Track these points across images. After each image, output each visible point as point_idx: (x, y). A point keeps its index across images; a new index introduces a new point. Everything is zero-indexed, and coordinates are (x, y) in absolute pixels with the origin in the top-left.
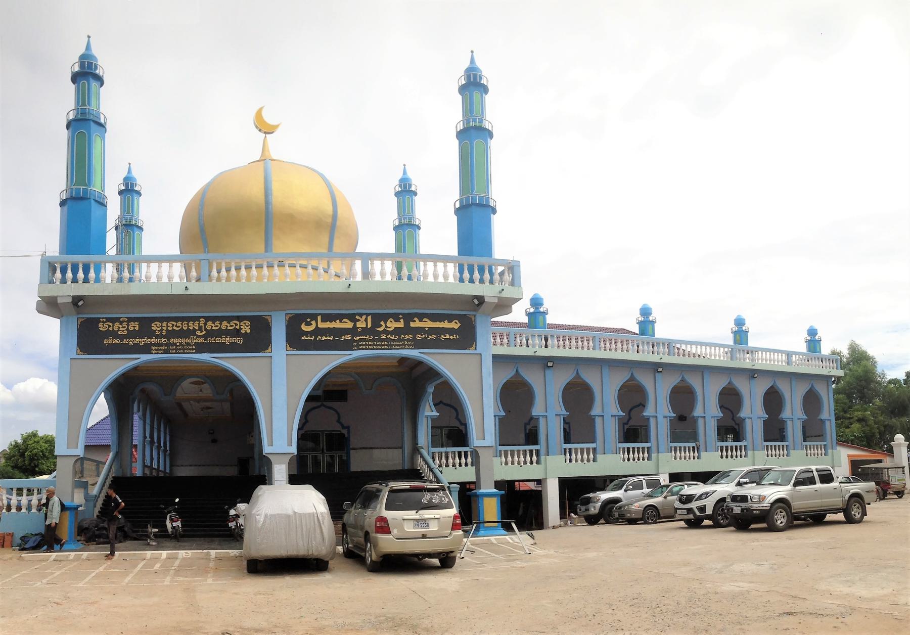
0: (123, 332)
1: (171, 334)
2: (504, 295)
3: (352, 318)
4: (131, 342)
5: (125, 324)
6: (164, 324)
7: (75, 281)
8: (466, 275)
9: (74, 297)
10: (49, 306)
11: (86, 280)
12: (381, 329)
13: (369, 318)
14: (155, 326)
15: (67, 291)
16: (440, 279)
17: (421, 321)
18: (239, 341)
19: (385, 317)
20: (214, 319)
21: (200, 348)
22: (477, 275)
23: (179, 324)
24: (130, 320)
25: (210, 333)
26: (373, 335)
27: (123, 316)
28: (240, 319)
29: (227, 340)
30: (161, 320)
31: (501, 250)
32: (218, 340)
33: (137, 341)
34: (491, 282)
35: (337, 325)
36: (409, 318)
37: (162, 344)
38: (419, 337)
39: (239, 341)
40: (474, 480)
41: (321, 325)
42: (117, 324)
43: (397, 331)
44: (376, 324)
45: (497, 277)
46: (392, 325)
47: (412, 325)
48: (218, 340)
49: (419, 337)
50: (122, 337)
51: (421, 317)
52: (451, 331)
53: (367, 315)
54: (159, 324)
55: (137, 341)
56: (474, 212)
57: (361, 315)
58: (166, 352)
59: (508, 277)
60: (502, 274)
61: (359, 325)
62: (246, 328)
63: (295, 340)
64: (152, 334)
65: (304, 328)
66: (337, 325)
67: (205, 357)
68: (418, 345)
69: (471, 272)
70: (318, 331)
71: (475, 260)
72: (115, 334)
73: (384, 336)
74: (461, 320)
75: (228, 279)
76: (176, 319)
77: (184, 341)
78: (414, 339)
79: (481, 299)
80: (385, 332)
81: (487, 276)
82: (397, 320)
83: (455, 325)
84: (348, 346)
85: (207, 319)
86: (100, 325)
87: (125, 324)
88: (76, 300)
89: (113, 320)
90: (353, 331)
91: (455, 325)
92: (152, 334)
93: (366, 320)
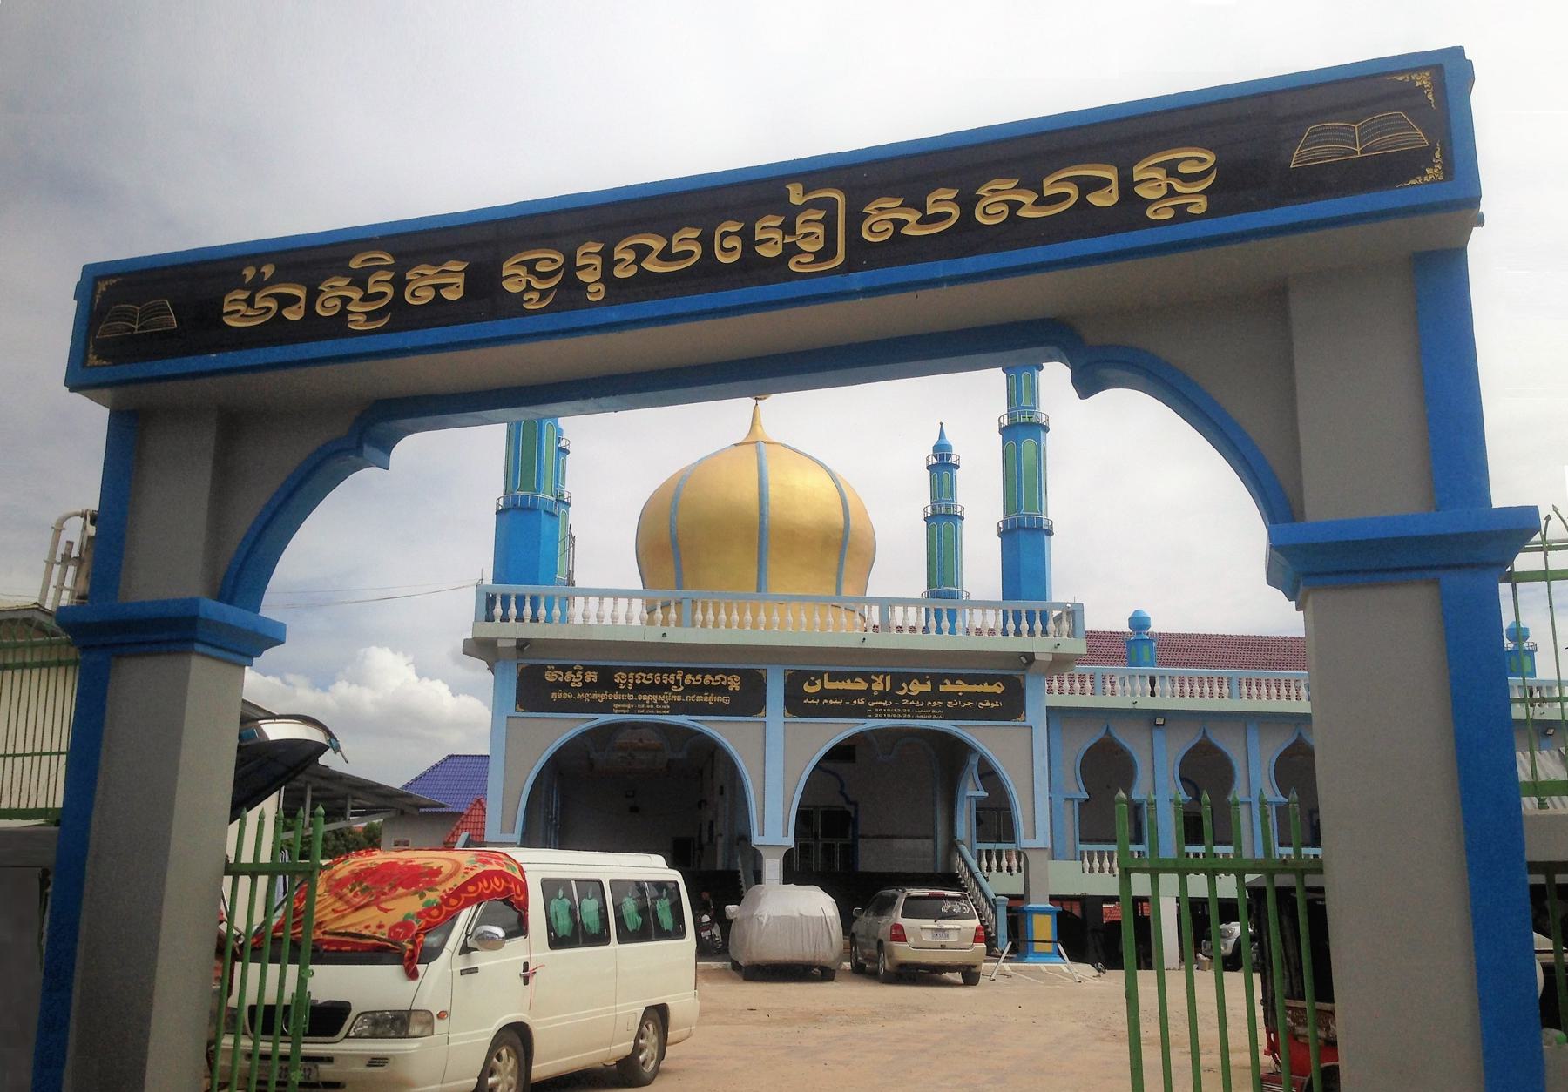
0: (576, 683)
1: (639, 688)
2: (1061, 650)
3: (866, 677)
4: (587, 697)
5: (579, 674)
6: (631, 675)
7: (520, 618)
8: (1011, 626)
9: (518, 640)
10: (481, 648)
11: (535, 619)
12: (902, 693)
13: (888, 678)
14: (619, 678)
15: (508, 632)
16: (982, 626)
17: (953, 683)
18: (725, 700)
19: (908, 678)
20: (694, 672)
21: (676, 709)
22: (1025, 625)
23: (650, 676)
24: (586, 669)
25: (690, 689)
26: (892, 700)
27: (578, 664)
28: (728, 672)
29: (710, 699)
30: (627, 670)
31: (1060, 591)
32: (699, 698)
33: (595, 696)
34: (1045, 632)
35: (848, 685)
36: (938, 679)
37: (627, 702)
38: (950, 704)
39: (725, 700)
40: (1022, 892)
41: (829, 685)
42: (569, 674)
43: (922, 696)
44: (897, 684)
45: (1051, 626)
46: (917, 688)
47: (942, 689)
48: (699, 698)
49: (950, 704)
50: (575, 691)
51: (953, 679)
52: (992, 697)
53: (886, 674)
54: (624, 675)
55: (595, 696)
56: (1024, 536)
57: (877, 674)
58: (632, 712)
59: (1065, 626)
60: (1058, 619)
61: (875, 687)
62: (734, 684)
63: (796, 704)
64: (614, 687)
65: (807, 688)
66: (848, 685)
67: (682, 720)
68: (949, 715)
69: (1017, 622)
70: (824, 693)
71: (1023, 605)
72: (565, 686)
73: (905, 702)
74: (1003, 686)
75: (716, 624)
76: (647, 670)
77: (655, 698)
78: (944, 707)
79: (1030, 657)
80: (907, 696)
81: (1038, 626)
82: (923, 682)
83: (997, 689)
84: (861, 713)
85: (686, 671)
86: (547, 674)
87: (579, 674)
88: (522, 645)
89: (564, 669)
90: (867, 694)
91: (997, 689)
92: (614, 687)
93: (884, 681)
